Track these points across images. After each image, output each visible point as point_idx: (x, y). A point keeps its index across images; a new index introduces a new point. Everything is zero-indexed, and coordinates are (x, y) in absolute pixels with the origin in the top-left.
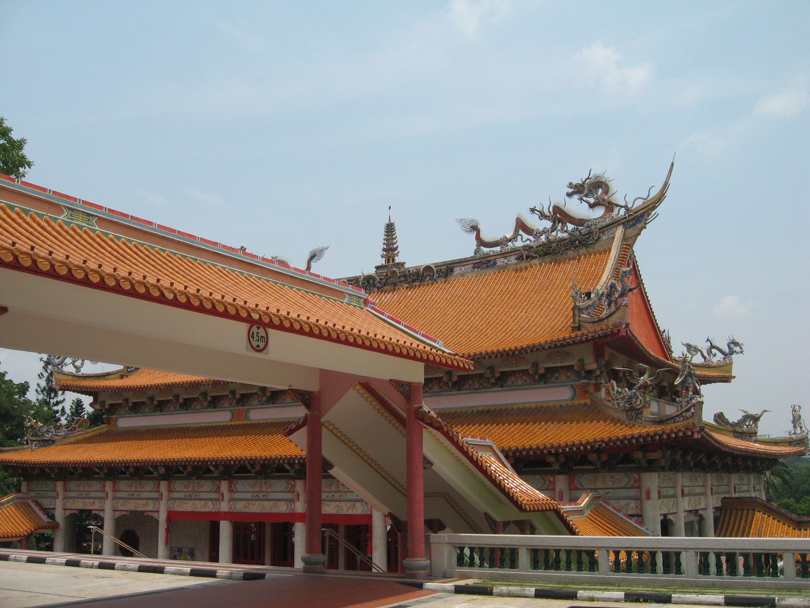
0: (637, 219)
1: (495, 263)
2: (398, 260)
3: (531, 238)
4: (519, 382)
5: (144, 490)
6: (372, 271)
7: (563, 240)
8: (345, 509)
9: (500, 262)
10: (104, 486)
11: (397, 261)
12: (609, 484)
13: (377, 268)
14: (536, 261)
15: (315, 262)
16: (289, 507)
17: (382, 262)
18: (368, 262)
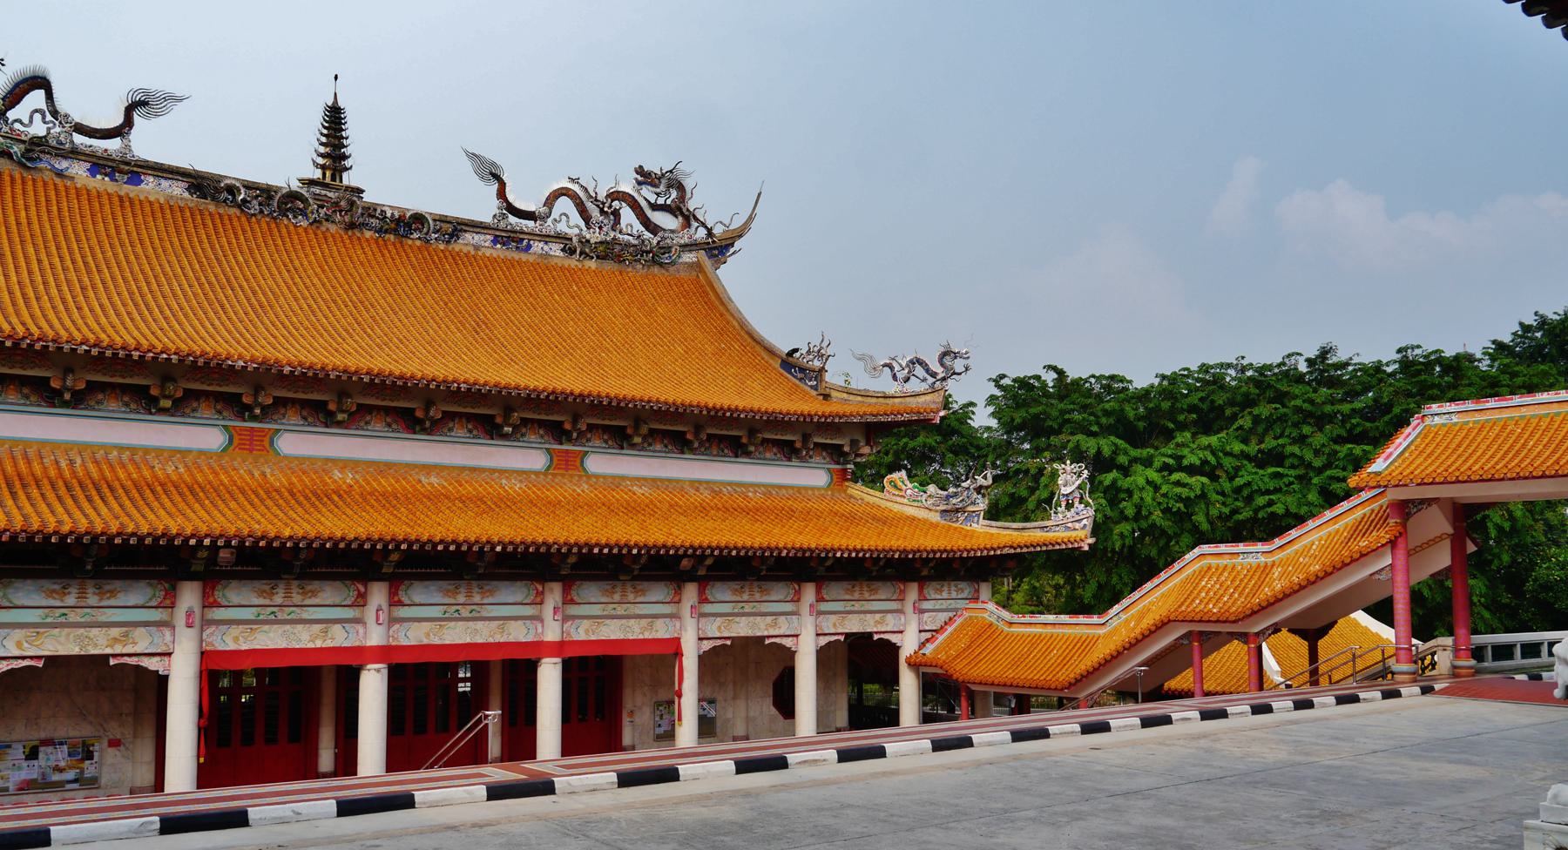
0: (719, 248)
1: (529, 246)
2: (348, 179)
3: (582, 224)
4: (768, 455)
5: (112, 602)
6: (295, 186)
7: (628, 245)
8: (637, 630)
9: (537, 247)
10: (977, 591)
11: (345, 182)
12: (954, 595)
13: (311, 183)
14: (592, 264)
15: (147, 116)
16: (532, 632)
17: (318, 174)
18: (289, 163)
